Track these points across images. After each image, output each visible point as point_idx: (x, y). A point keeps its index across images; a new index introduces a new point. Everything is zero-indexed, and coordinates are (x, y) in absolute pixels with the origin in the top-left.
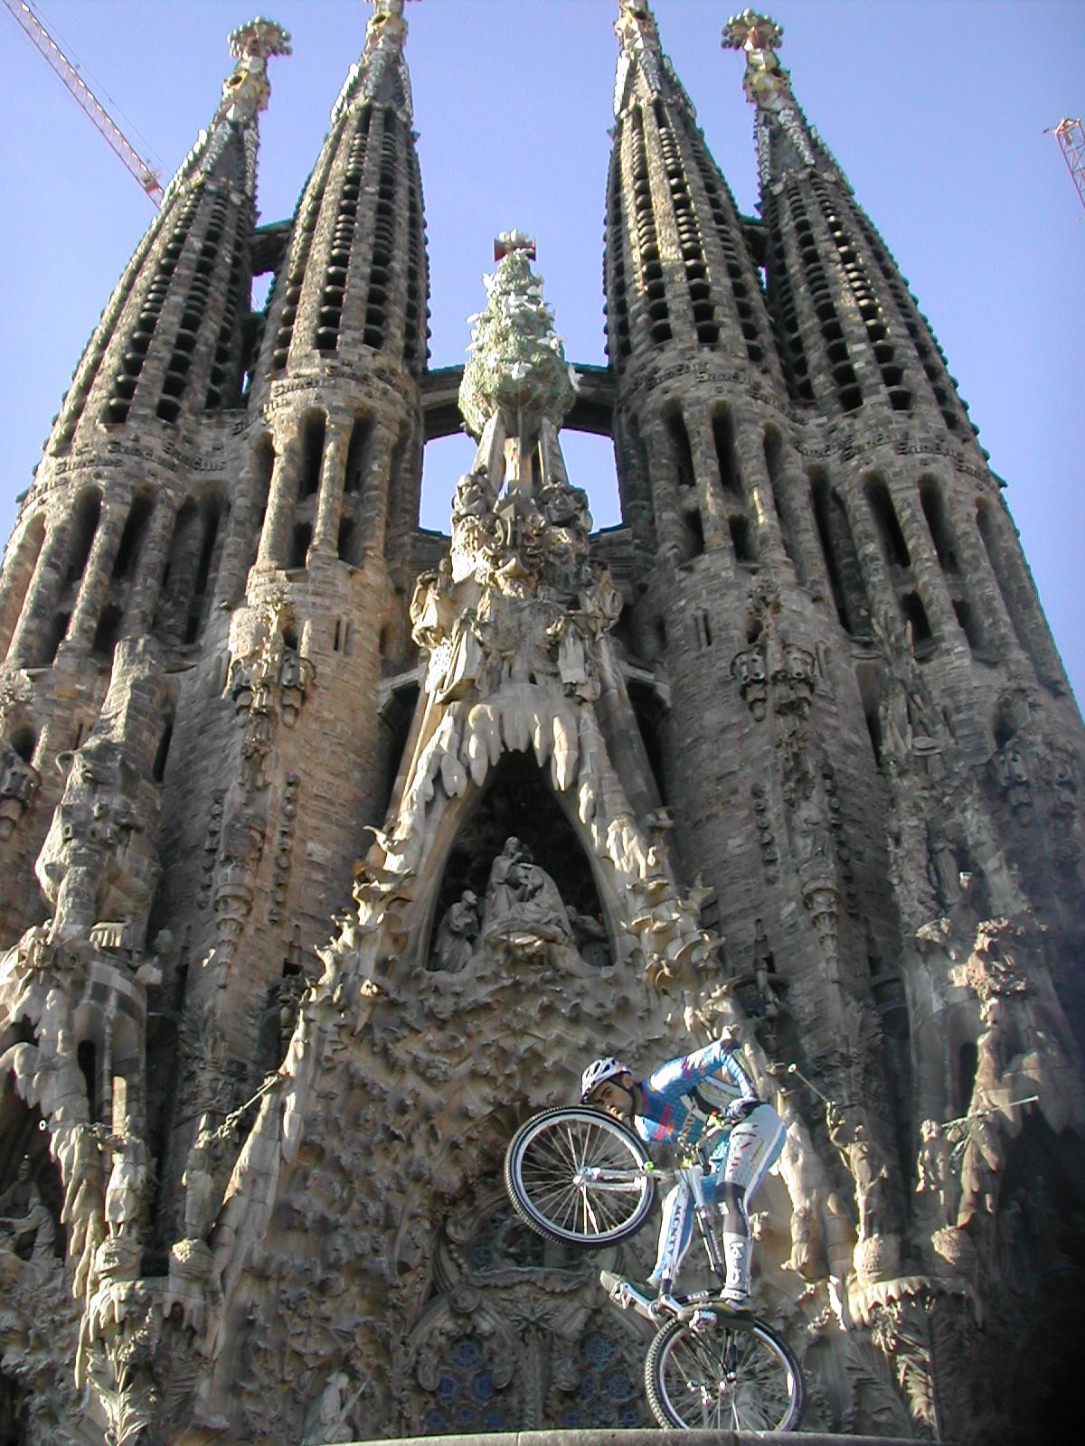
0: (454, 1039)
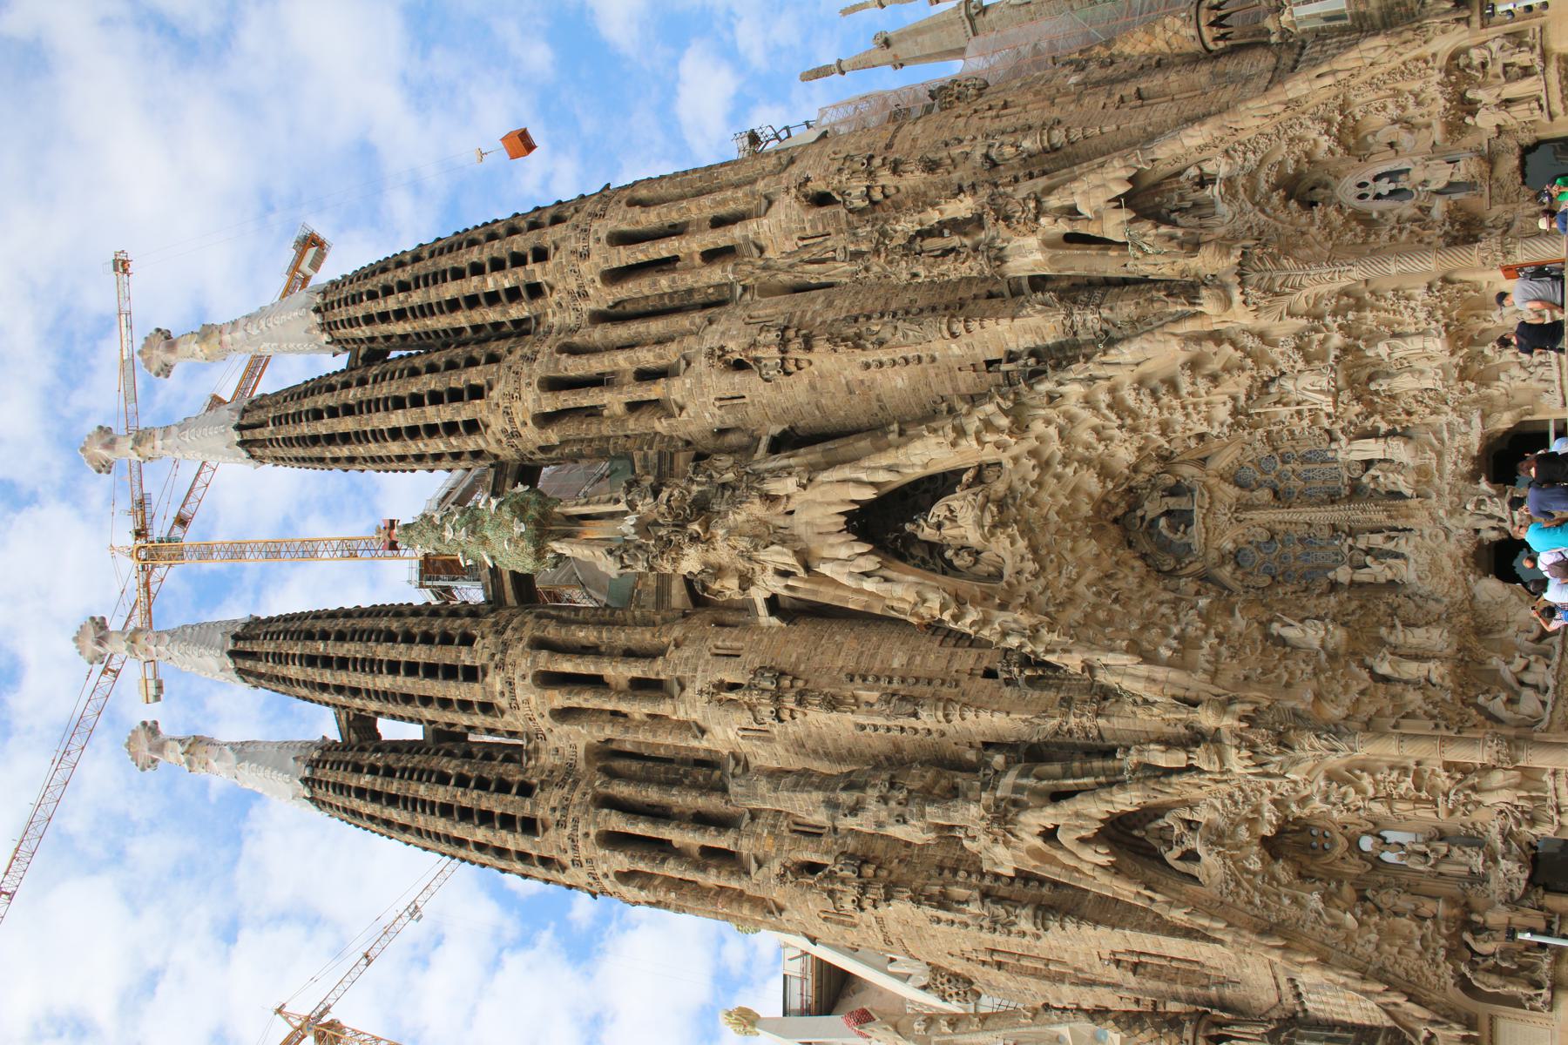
0: (1052, 561)
